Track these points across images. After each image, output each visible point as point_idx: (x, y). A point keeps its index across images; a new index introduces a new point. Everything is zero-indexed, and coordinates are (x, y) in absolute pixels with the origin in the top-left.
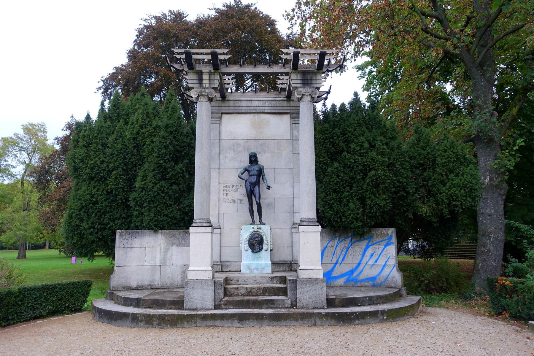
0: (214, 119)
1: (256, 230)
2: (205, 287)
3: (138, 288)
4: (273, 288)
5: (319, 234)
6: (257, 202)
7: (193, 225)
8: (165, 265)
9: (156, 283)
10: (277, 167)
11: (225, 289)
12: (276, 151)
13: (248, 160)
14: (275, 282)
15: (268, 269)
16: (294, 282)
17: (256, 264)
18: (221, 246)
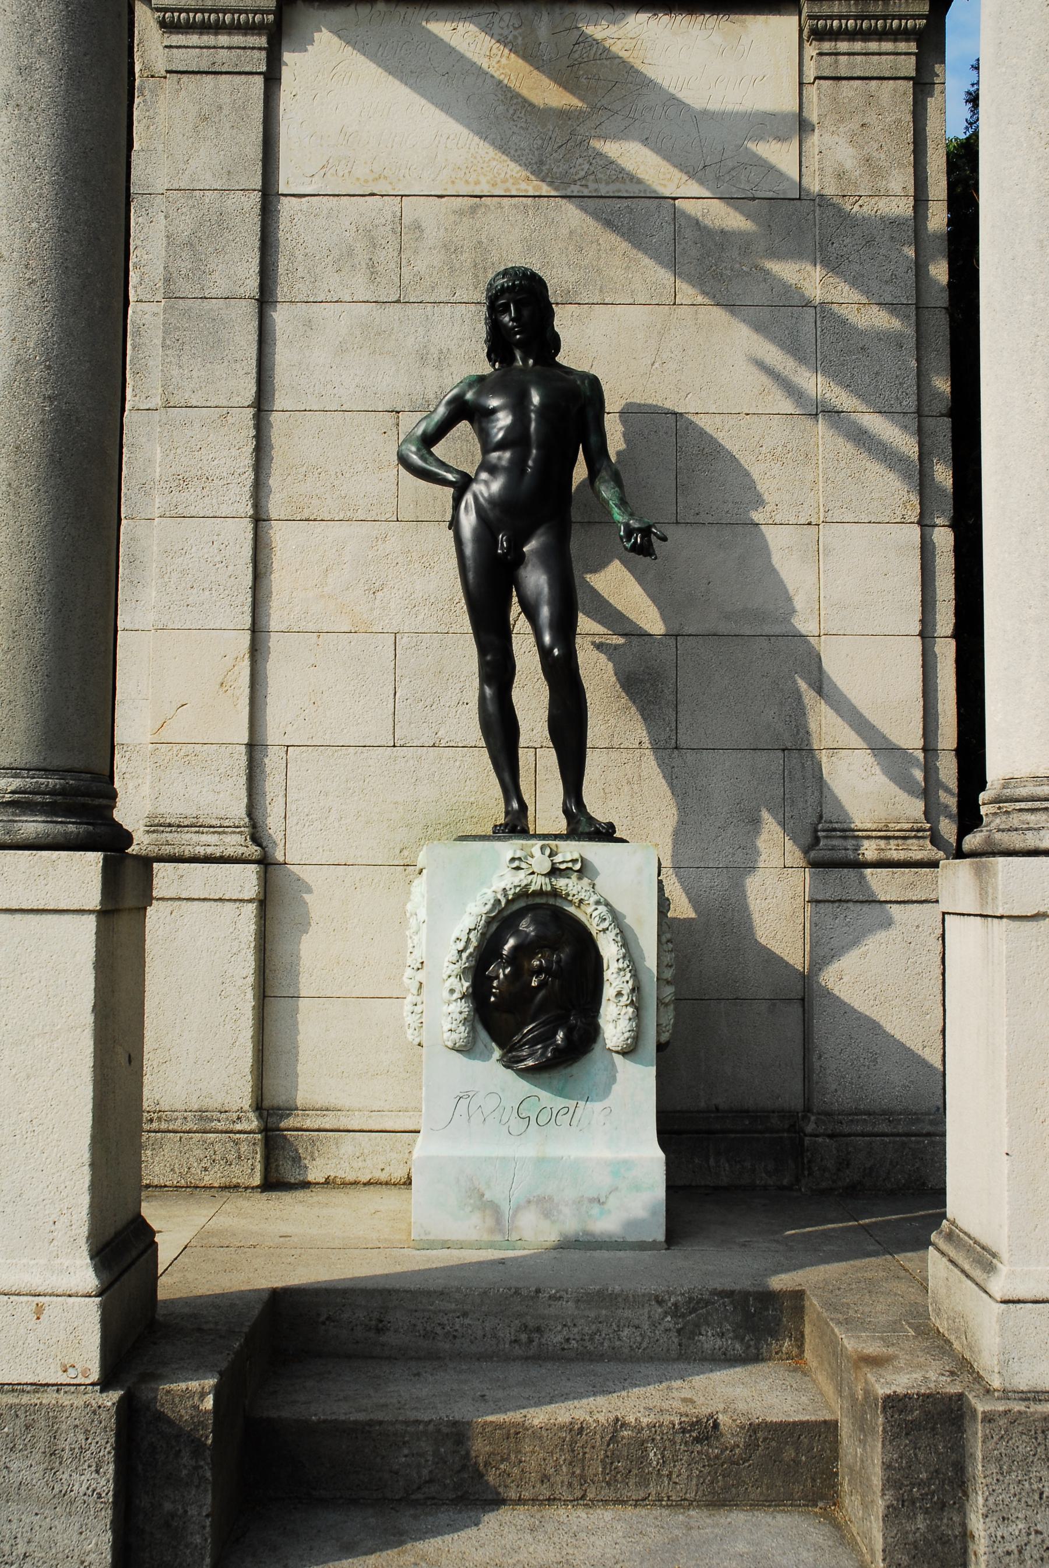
0: (223, 40)
1: (539, 883)
6: (544, 653)
17: (541, 1161)
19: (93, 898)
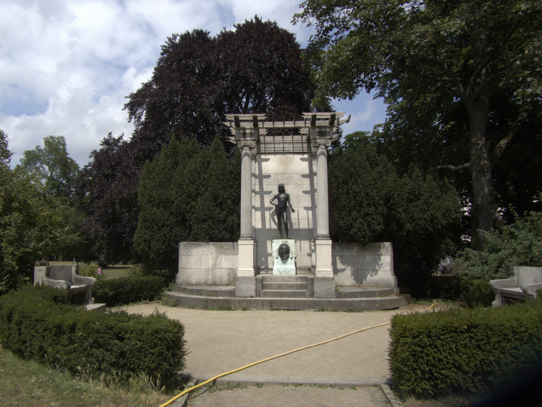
2: (250, 282)
3: (196, 284)
4: (297, 284)
5: (331, 246)
7: (241, 239)
8: (216, 268)
9: (209, 281)
10: (299, 195)
11: (262, 284)
12: (299, 183)
13: (278, 190)
14: (298, 280)
15: (293, 273)
16: (312, 280)
18: (257, 255)
19: (253, 243)
